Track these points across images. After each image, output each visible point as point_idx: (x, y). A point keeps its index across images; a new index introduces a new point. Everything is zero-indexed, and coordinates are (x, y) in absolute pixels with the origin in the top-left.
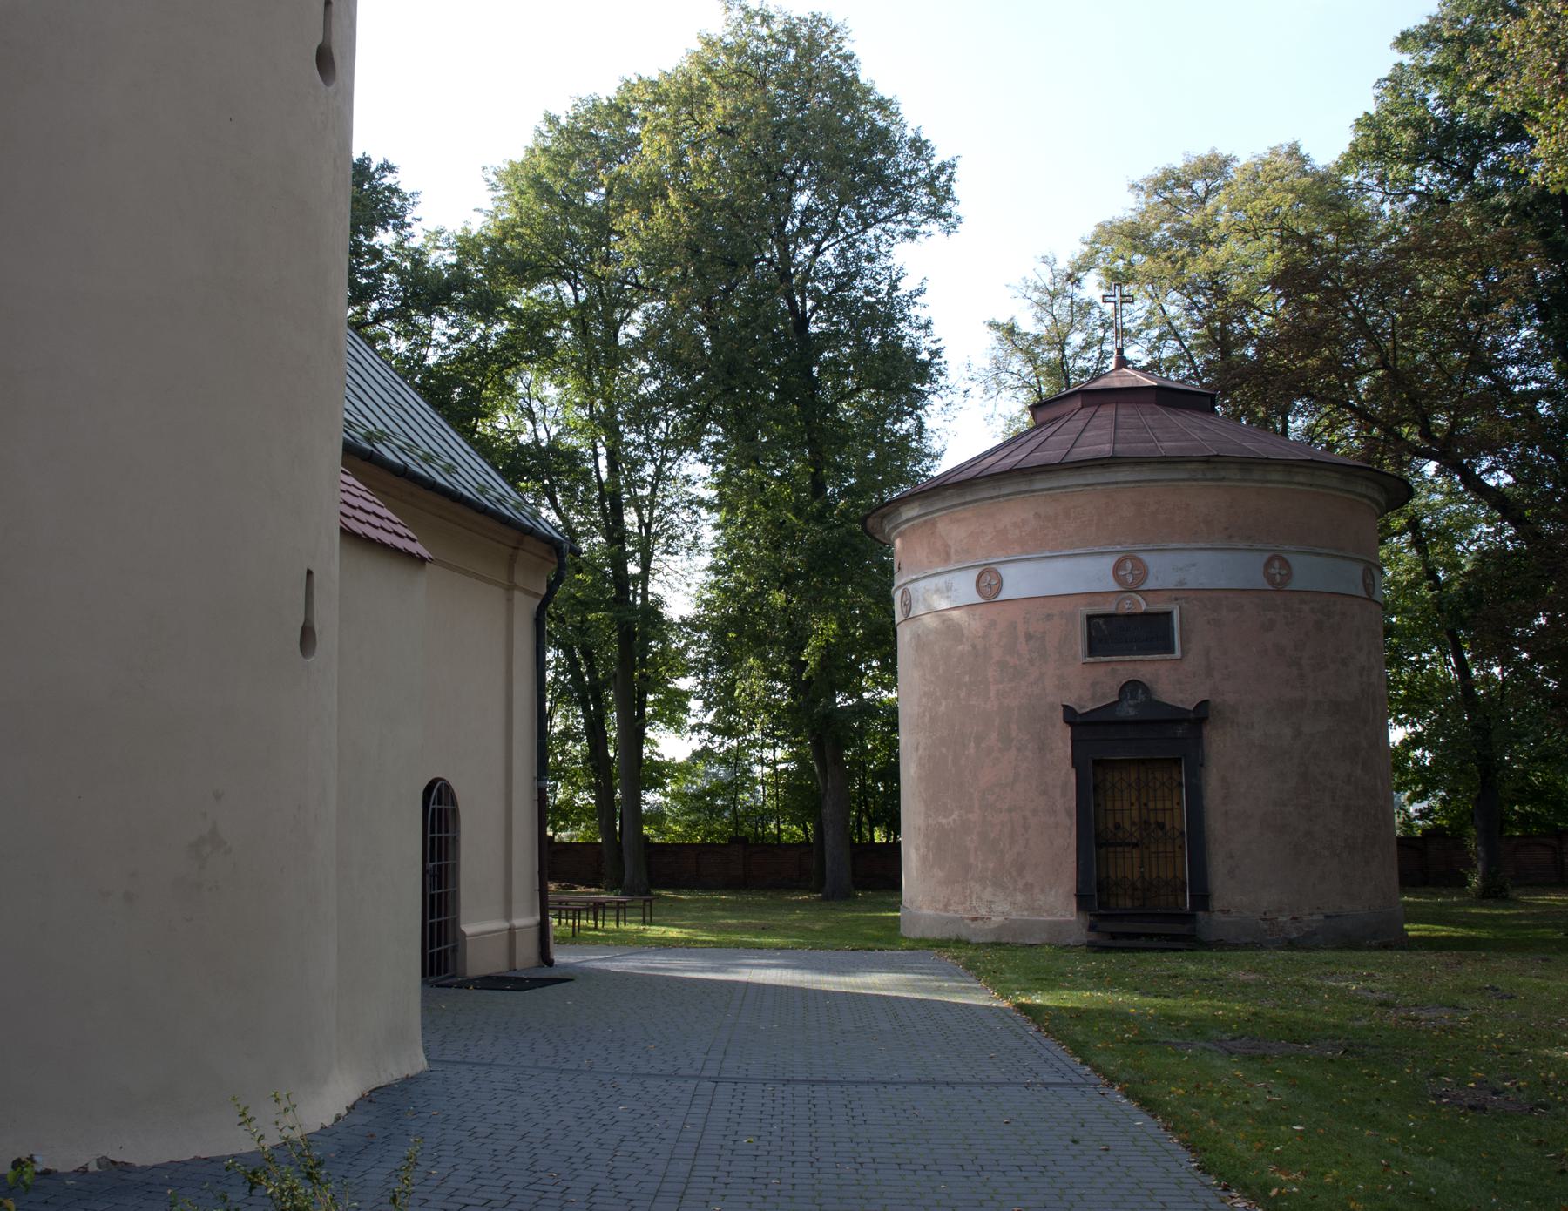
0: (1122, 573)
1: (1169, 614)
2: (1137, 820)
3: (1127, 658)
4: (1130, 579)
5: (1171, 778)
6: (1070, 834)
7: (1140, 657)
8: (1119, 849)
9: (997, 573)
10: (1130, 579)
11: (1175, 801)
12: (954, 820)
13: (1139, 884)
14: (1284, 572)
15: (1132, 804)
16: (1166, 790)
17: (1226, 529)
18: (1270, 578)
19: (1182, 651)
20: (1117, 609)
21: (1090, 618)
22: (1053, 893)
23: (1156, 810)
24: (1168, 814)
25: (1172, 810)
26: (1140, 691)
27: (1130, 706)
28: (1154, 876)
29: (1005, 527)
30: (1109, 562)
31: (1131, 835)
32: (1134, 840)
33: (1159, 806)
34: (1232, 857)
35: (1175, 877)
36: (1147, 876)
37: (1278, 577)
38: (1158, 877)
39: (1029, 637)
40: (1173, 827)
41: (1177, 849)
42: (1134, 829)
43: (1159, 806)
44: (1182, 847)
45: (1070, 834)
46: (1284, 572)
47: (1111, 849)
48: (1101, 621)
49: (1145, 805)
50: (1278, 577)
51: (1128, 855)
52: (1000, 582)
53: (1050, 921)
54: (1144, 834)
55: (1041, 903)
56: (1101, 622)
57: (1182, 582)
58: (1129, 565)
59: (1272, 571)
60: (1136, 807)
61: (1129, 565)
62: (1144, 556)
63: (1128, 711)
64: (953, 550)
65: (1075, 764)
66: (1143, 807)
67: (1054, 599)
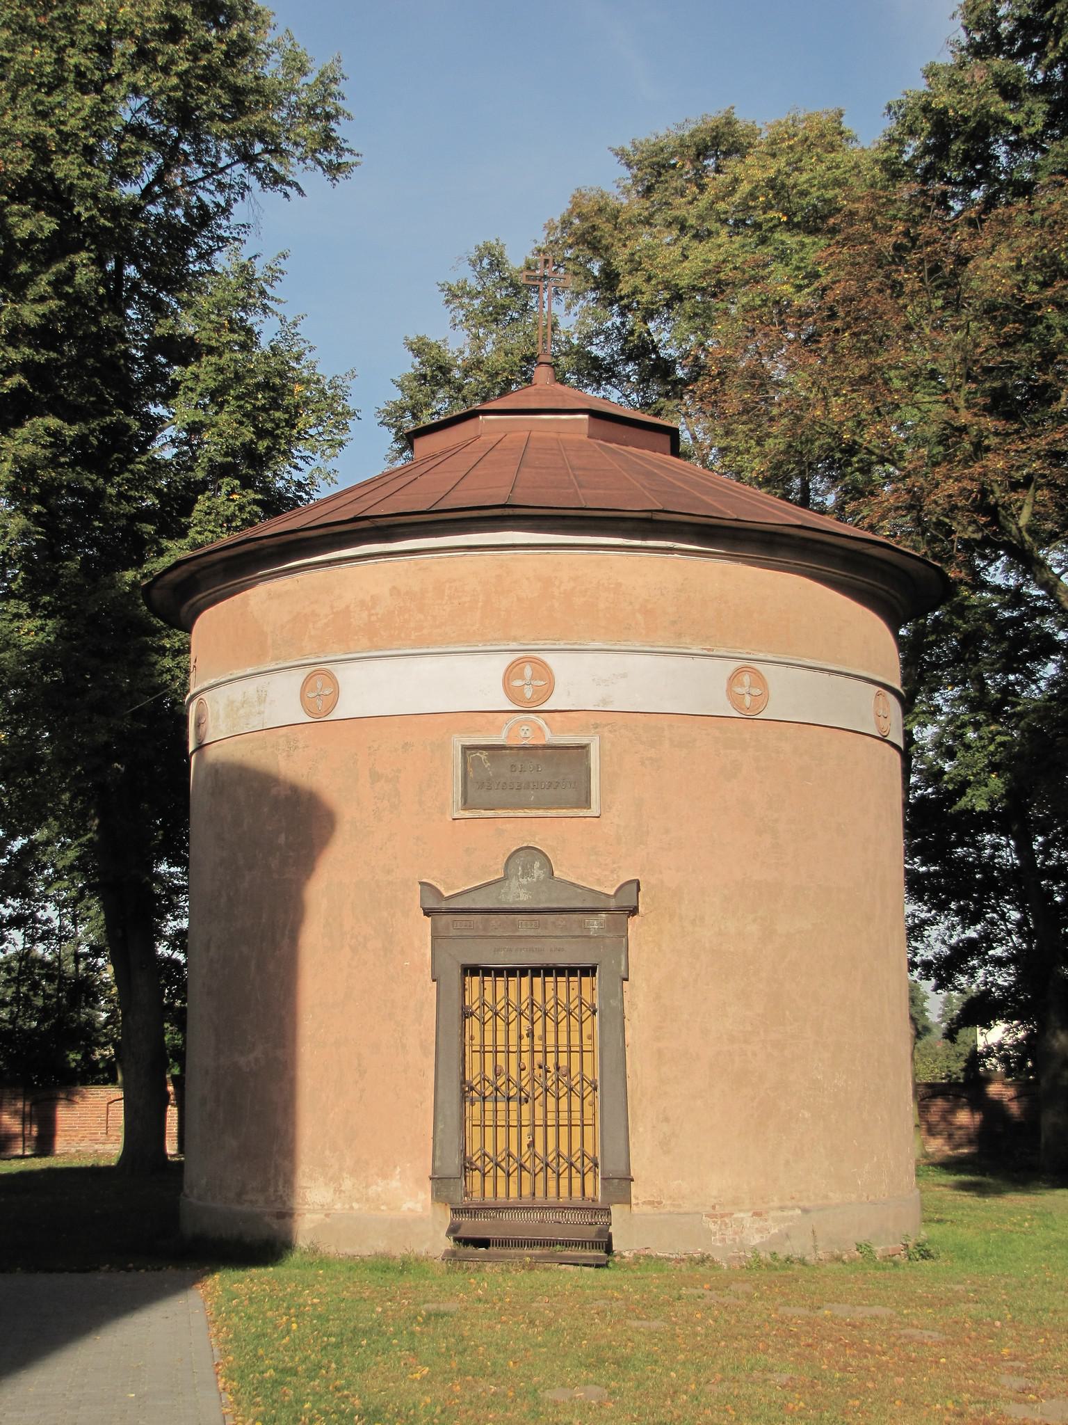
0: (518, 683)
1: (584, 748)
3: (520, 813)
4: (528, 693)
7: (541, 813)
9: (331, 677)
10: (528, 693)
12: (257, 1060)
14: (756, 691)
17: (674, 623)
18: (735, 700)
21: (466, 749)
26: (537, 865)
27: (521, 886)
29: (348, 607)
30: (500, 663)
34: (667, 1120)
37: (748, 699)
39: (375, 777)
44: (593, 1104)
46: (756, 691)
48: (483, 755)
50: (748, 698)
52: (336, 692)
55: (380, 1189)
56: (483, 757)
57: (604, 701)
58: (528, 671)
59: (739, 690)
61: (528, 671)
63: (518, 894)
64: (269, 642)
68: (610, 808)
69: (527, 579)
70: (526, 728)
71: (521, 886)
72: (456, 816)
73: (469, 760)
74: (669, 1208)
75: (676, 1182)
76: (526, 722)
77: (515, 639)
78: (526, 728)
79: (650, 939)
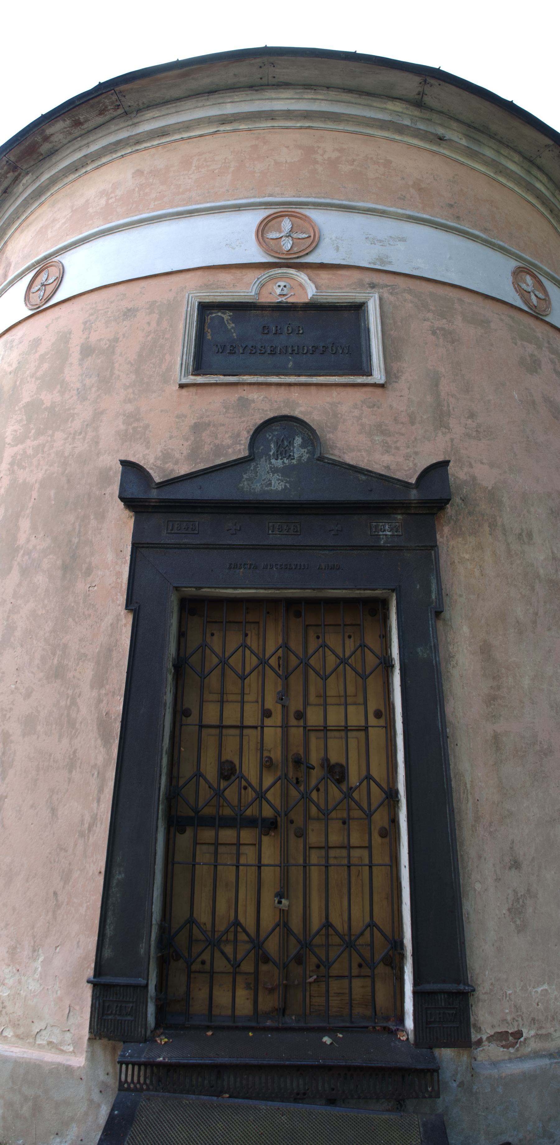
2: (277, 755)
5: (363, 646)
6: (101, 790)
7: (303, 379)
8: (227, 835)
11: (372, 706)
13: (272, 946)
15: (267, 714)
16: (350, 674)
19: (388, 371)
20: (258, 294)
22: (38, 964)
23: (325, 729)
24: (354, 740)
25: (366, 729)
26: (298, 441)
27: (275, 470)
28: (316, 922)
31: (261, 796)
32: (268, 812)
33: (335, 718)
34: (516, 865)
35: (372, 925)
36: (296, 923)
38: (328, 925)
40: (369, 777)
41: (376, 839)
42: (268, 781)
43: (335, 718)
45: (101, 790)
47: (207, 834)
48: (226, 316)
49: (300, 715)
51: (249, 855)
53: (17, 1063)
54: (294, 793)
57: (382, 262)
60: (277, 718)
62: (315, 215)
65: (129, 605)
66: (293, 721)
67: (143, 283)
68: (397, 377)
69: (287, 147)
70: (282, 284)
71: (275, 470)
72: (184, 381)
73: (208, 320)
74: (534, 1045)
75: (539, 990)
76: (282, 277)
77: (270, 195)
78: (282, 284)
79: (467, 556)
